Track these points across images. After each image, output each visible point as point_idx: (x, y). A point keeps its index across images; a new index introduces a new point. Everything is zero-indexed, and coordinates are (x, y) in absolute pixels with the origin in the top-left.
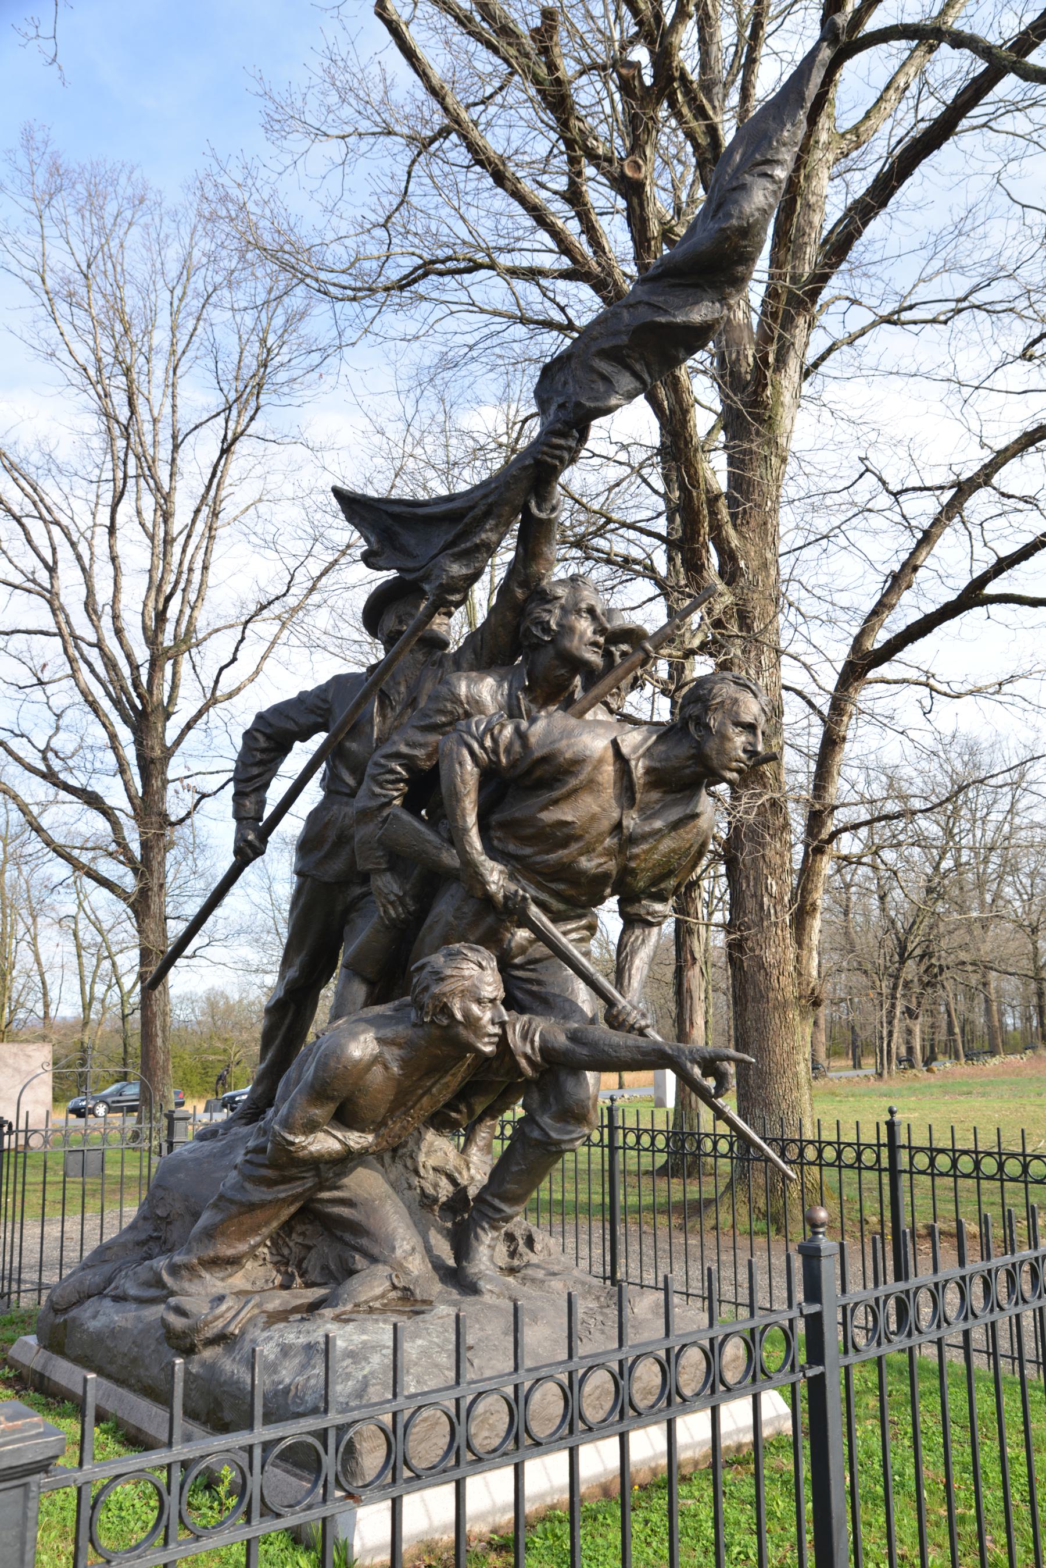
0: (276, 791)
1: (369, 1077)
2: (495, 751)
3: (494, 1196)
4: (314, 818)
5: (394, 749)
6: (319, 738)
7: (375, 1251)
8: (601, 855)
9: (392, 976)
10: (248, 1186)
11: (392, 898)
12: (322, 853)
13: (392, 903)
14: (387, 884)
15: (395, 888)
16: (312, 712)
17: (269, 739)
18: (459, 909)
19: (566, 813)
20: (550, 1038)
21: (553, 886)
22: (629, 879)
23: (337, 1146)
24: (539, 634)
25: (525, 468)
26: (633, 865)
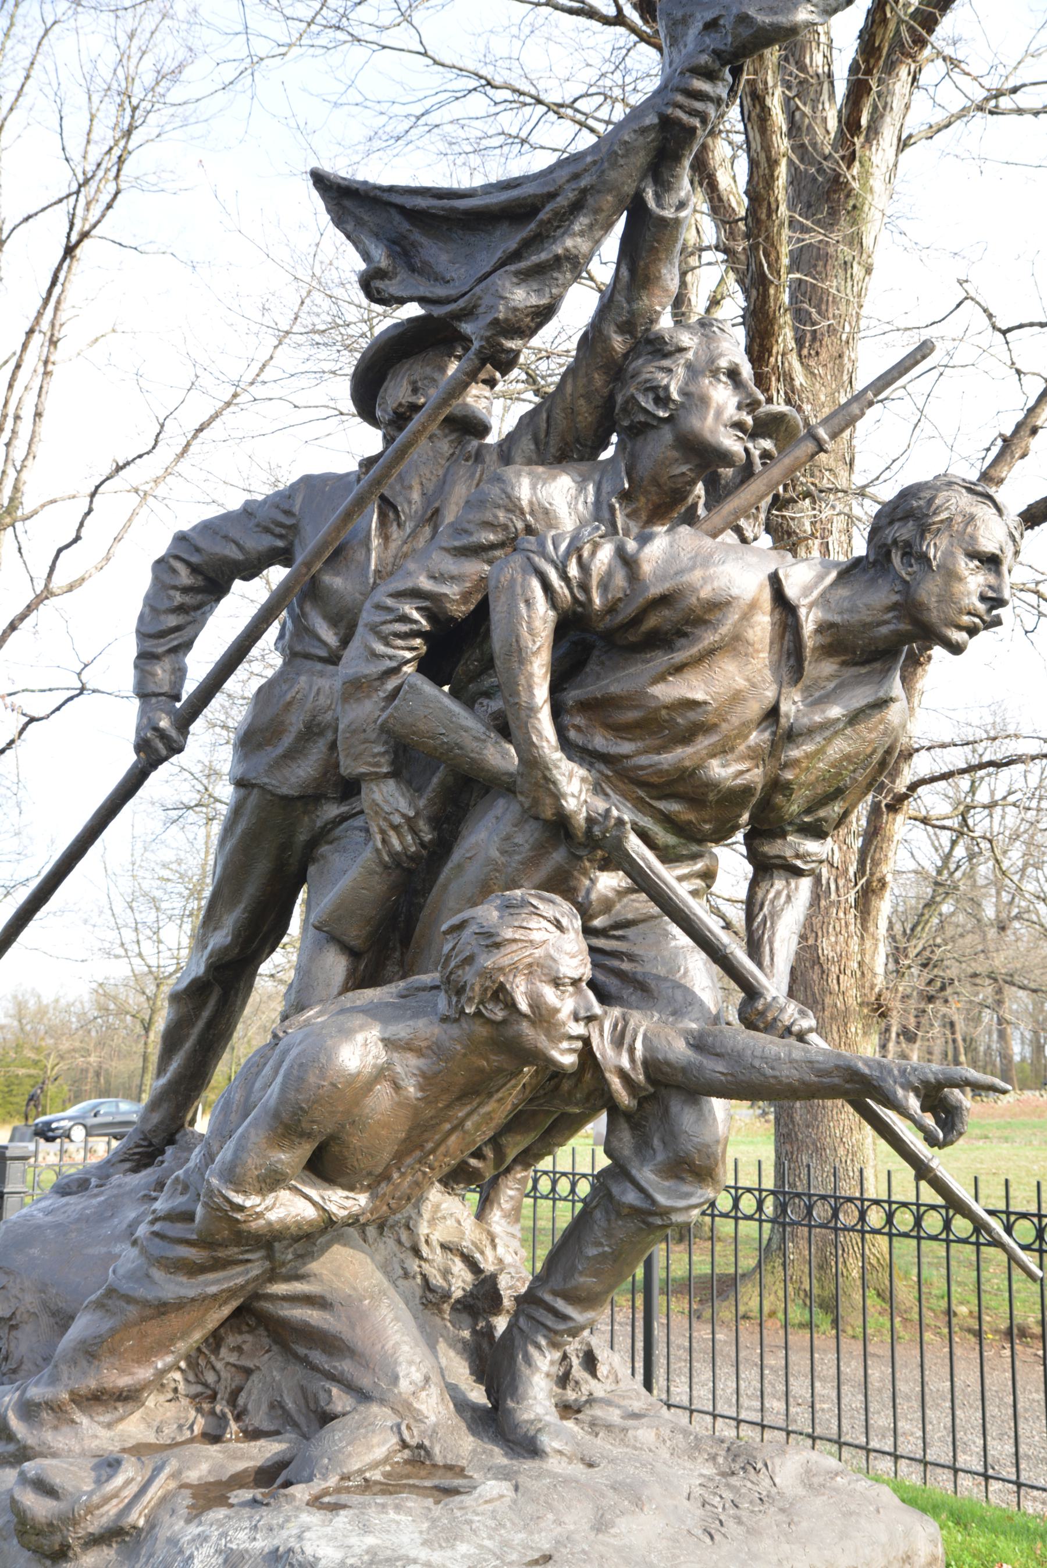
0: (200, 661)
1: (370, 1101)
2: (585, 587)
3: (556, 1294)
4: (265, 694)
5: (409, 584)
6: (277, 574)
7: (365, 1381)
8: (742, 758)
9: (385, 945)
10: (157, 1274)
11: (397, 819)
12: (280, 750)
13: (396, 828)
14: (389, 798)
15: (403, 805)
16: (267, 530)
17: (197, 573)
18: (508, 838)
19: (693, 687)
20: (661, 1044)
21: (662, 805)
22: (779, 799)
23: (310, 1213)
24: (650, 406)
25: (644, 131)
26: (789, 775)
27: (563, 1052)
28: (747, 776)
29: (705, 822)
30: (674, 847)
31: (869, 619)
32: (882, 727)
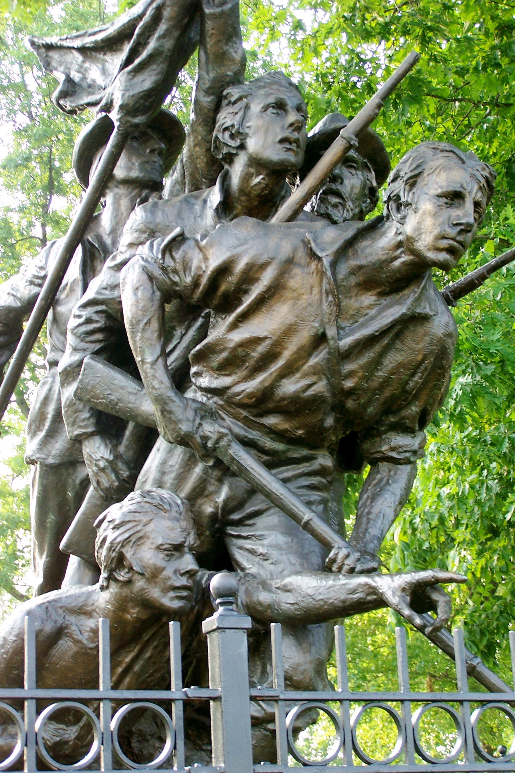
8: (305, 376)
11: (102, 464)
27: (172, 599)
28: (314, 388)
29: (298, 428)
30: (284, 452)
31: (384, 258)
32: (427, 338)
